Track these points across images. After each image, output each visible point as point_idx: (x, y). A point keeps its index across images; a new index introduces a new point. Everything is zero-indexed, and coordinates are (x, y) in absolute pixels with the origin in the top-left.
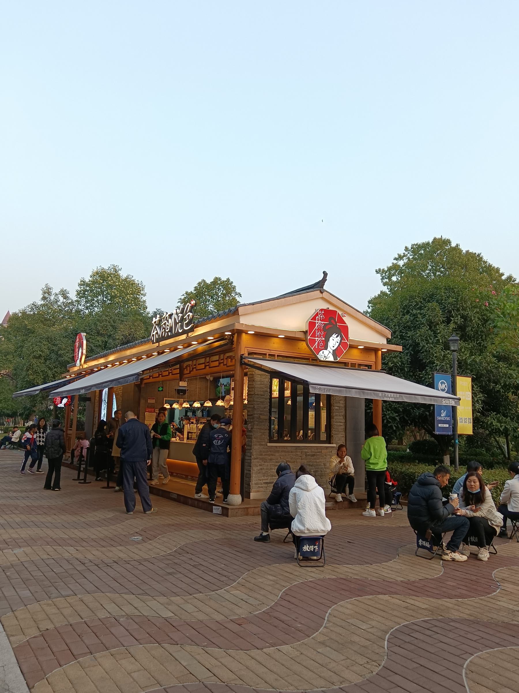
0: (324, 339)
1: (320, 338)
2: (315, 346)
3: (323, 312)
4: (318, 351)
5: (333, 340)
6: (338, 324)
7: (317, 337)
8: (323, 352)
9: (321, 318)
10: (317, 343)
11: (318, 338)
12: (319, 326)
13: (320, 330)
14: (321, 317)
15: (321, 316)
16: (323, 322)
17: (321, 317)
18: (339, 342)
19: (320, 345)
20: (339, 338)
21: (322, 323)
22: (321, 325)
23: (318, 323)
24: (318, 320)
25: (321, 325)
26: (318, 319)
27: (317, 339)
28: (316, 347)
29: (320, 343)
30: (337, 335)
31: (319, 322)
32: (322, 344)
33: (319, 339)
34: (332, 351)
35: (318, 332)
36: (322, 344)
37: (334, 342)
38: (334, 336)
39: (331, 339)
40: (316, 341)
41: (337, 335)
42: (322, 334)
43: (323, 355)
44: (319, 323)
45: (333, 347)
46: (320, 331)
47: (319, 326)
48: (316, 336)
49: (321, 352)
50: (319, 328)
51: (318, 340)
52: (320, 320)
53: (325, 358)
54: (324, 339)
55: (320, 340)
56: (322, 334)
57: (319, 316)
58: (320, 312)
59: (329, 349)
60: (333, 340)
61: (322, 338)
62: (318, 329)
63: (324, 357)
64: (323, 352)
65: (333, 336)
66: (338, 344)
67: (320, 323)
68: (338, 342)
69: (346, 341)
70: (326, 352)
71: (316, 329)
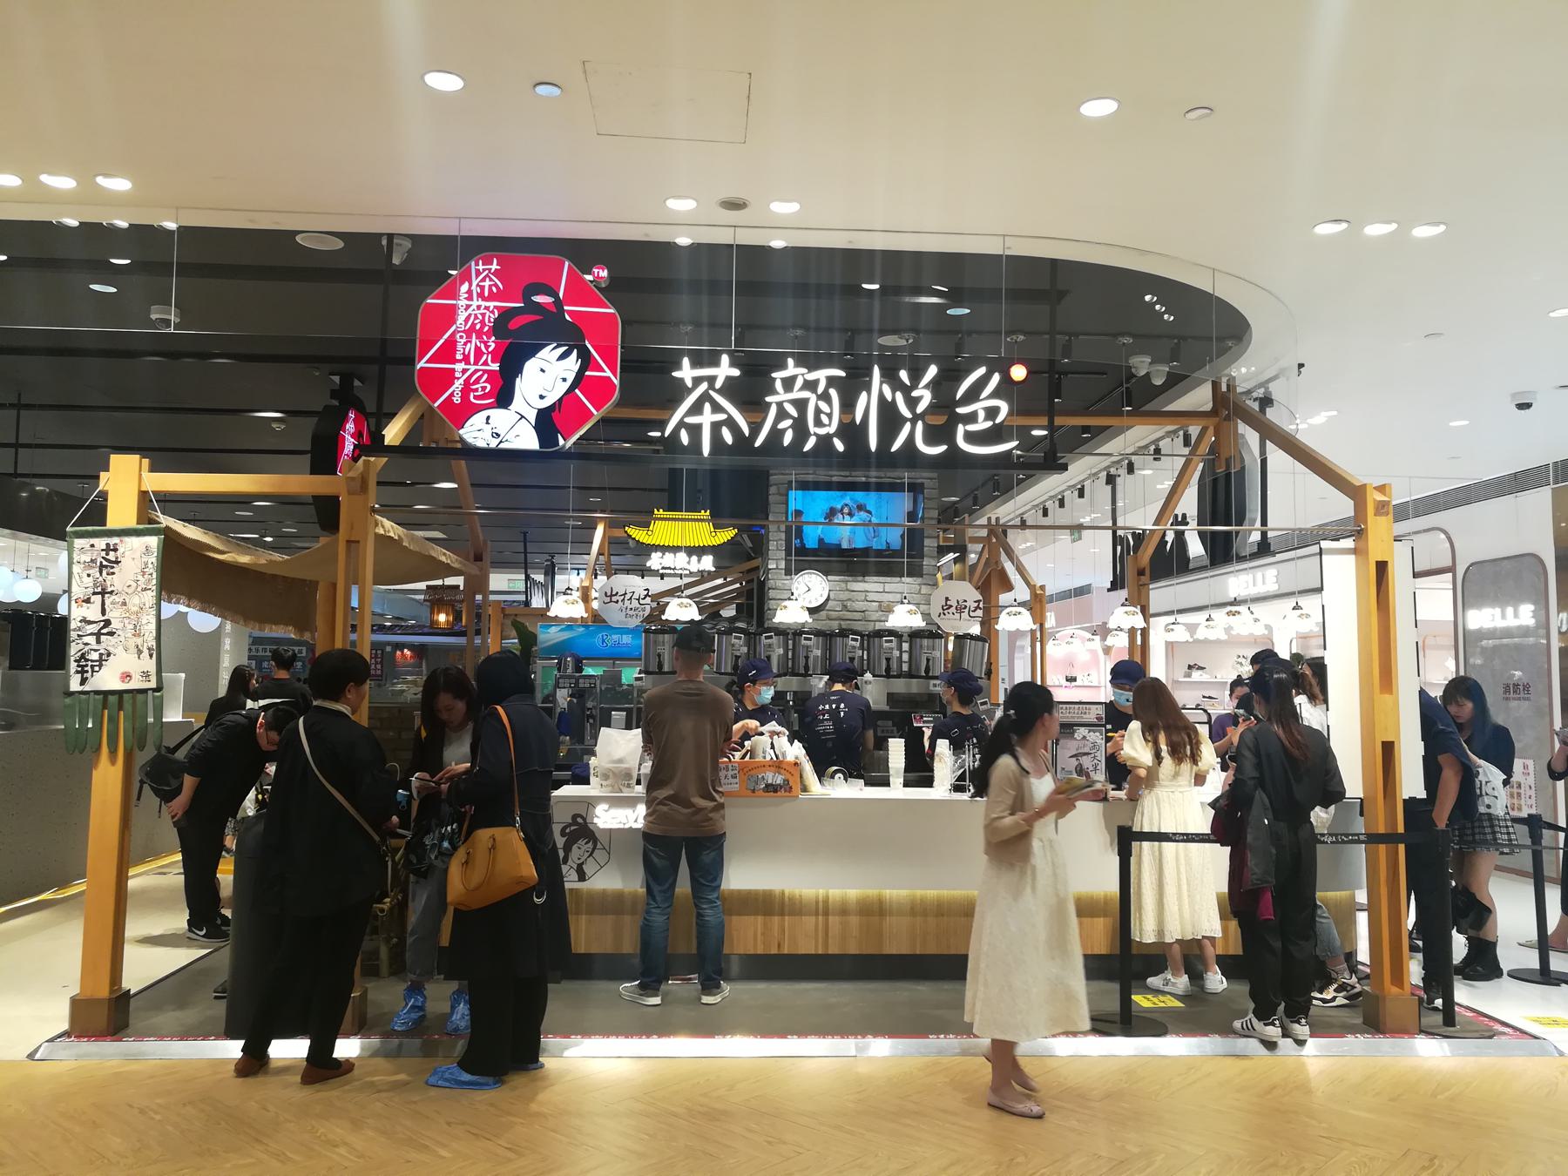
0: (495, 367)
1: (476, 363)
2: (452, 394)
3: (494, 267)
4: (463, 412)
5: (542, 371)
6: (566, 308)
7: (460, 361)
8: (488, 418)
9: (482, 288)
11: (468, 363)
12: (476, 317)
13: (479, 334)
14: (487, 283)
15: (483, 280)
16: (492, 304)
17: (487, 283)
18: (571, 377)
19: (476, 390)
20: (572, 364)
21: (487, 308)
22: (483, 315)
23: (468, 307)
24: (470, 298)
26: (470, 292)
27: (459, 367)
28: (457, 399)
29: (477, 381)
30: (564, 348)
31: (475, 303)
32: (484, 388)
33: (473, 368)
34: (532, 416)
36: (484, 388)
37: (546, 380)
38: (549, 354)
39: (531, 366)
40: (457, 375)
41: (564, 348)
42: (487, 347)
43: (488, 429)
44: (474, 307)
45: (542, 397)
47: (476, 317)
48: (459, 357)
49: (477, 420)
50: (474, 325)
51: (464, 371)
54: (495, 367)
55: (476, 371)
56: (487, 347)
57: (475, 283)
58: (481, 267)
59: (518, 403)
60: (542, 371)
61: (485, 363)
62: (469, 333)
64: (488, 418)
66: (567, 385)
67: (479, 307)
68: (564, 380)
69: (608, 373)
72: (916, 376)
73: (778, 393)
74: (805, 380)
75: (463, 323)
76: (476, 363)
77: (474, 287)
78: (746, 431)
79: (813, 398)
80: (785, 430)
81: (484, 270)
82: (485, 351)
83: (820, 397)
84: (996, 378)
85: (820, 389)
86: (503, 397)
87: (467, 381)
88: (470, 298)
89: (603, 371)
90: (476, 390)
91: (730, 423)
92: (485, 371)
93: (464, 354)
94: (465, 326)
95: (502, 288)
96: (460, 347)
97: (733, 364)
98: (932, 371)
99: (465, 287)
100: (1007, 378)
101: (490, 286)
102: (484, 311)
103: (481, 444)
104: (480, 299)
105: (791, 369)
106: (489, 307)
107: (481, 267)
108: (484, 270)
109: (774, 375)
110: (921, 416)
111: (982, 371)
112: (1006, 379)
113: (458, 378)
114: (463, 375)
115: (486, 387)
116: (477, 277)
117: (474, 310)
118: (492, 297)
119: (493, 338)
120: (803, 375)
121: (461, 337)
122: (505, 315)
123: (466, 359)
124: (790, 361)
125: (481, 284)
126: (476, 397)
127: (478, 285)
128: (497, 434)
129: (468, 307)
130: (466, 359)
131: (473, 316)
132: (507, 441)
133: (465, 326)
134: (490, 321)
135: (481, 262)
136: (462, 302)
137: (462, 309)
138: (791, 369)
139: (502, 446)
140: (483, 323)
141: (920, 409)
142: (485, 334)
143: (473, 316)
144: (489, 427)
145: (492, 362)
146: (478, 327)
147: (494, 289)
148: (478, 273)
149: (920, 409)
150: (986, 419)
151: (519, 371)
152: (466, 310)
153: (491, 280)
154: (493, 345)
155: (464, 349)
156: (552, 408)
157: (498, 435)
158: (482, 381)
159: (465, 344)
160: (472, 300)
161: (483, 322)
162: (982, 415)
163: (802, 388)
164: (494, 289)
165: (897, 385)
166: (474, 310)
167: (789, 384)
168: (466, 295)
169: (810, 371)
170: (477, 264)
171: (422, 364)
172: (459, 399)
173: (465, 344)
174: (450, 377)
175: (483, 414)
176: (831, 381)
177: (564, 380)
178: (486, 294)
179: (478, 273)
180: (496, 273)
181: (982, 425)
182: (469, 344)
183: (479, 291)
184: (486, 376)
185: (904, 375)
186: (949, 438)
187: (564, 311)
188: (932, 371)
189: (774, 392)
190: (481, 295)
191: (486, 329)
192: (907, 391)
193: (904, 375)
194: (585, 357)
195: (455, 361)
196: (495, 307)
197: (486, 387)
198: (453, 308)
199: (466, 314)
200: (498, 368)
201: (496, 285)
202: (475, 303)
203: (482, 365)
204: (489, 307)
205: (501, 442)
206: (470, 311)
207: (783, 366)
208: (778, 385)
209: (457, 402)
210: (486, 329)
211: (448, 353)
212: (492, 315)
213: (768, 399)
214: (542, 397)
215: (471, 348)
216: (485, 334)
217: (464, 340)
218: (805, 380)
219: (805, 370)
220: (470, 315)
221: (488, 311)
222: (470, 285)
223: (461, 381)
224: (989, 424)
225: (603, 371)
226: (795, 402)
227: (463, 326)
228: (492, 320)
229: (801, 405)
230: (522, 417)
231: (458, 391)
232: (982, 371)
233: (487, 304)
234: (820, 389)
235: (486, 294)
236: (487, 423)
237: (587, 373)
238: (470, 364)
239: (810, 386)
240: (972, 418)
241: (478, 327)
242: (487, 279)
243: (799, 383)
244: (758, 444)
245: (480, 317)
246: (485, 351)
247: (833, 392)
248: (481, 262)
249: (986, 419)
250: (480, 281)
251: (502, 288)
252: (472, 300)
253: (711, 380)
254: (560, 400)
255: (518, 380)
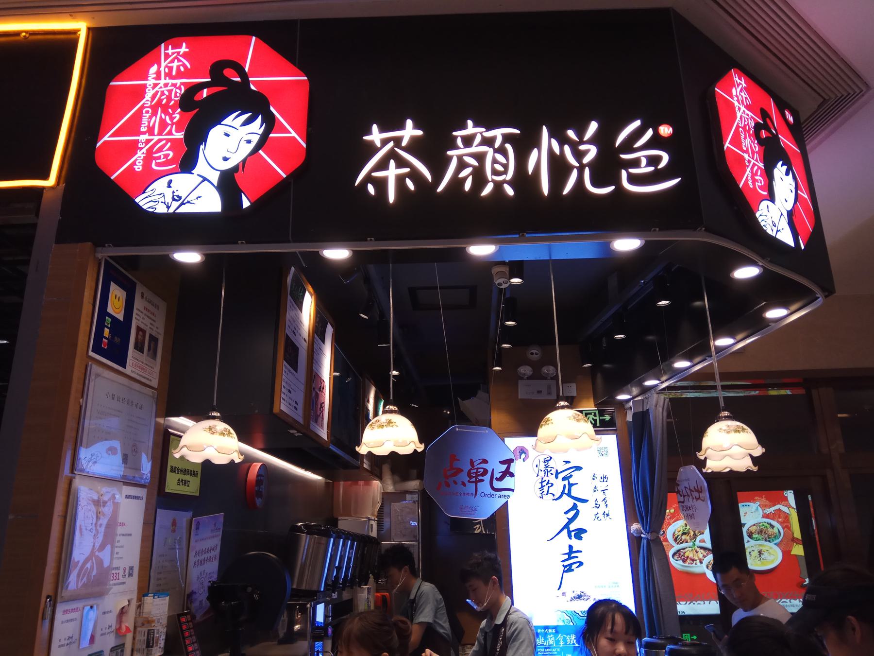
1: (160, 134)
2: (134, 163)
5: (227, 135)
7: (144, 133)
8: (170, 182)
9: (171, 69)
10: (140, 154)
12: (163, 93)
14: (176, 64)
15: (172, 61)
16: (178, 82)
17: (176, 64)
19: (159, 158)
20: (257, 127)
21: (174, 85)
23: (155, 85)
25: (170, 91)
27: (143, 138)
28: (139, 167)
29: (160, 150)
33: (156, 138)
34: (215, 177)
35: (154, 114)
36: (166, 156)
38: (234, 120)
39: (216, 134)
40: (140, 145)
44: (162, 85)
45: (226, 159)
46: (166, 112)
47: (163, 93)
48: (143, 129)
49: (160, 185)
50: (160, 100)
51: (148, 141)
52: (166, 75)
53: (175, 204)
55: (160, 141)
56: (172, 119)
57: (163, 64)
59: (201, 167)
60: (227, 135)
61: (170, 133)
63: (169, 199)
65: (228, 120)
66: (251, 146)
67: (166, 85)
69: (293, 134)
70: (183, 183)
71: (143, 107)
72: (580, 133)
73: (458, 148)
74: (483, 137)
75: (150, 99)
76: (160, 134)
77: (162, 69)
78: (428, 176)
79: (490, 151)
80: (465, 178)
81: (173, 53)
82: (170, 122)
83: (496, 151)
84: (650, 133)
85: (497, 144)
86: (187, 163)
87: (150, 152)
88: (158, 76)
89: (290, 133)
90: (159, 158)
91: (415, 175)
92: (168, 141)
93: (148, 126)
94: (152, 102)
95: (189, 66)
96: (145, 121)
97: (416, 126)
98: (593, 126)
99: (154, 69)
100: (656, 133)
101: (178, 67)
102: (172, 88)
103: (161, 209)
104: (167, 78)
105: (471, 128)
106: (176, 84)
107: (170, 51)
108: (173, 53)
109: (455, 133)
110: (588, 165)
111: (637, 123)
112: (656, 133)
113: (141, 149)
114: (146, 145)
115: (169, 155)
116: (165, 60)
117: (161, 88)
118: (179, 75)
119: (179, 110)
120: (481, 133)
121: (147, 112)
122: (193, 90)
123: (150, 131)
124: (470, 123)
125: (169, 65)
126: (158, 165)
127: (167, 66)
128: (178, 196)
129: (155, 85)
130: (150, 131)
131: (159, 94)
132: (188, 202)
133: (152, 102)
134: (176, 96)
135: (170, 47)
136: (151, 82)
137: (150, 88)
138: (471, 128)
139: (183, 210)
140: (169, 98)
141: (587, 160)
142: (170, 107)
143: (159, 94)
144: (171, 190)
145: (177, 131)
146: (164, 102)
147: (182, 69)
148: (167, 56)
149: (587, 160)
150: (648, 165)
151: (204, 139)
152: (153, 88)
153: (179, 61)
154: (178, 117)
155: (149, 122)
156: (235, 169)
157: (180, 198)
158: (164, 150)
159: (150, 118)
160: (160, 79)
161: (169, 98)
162: (644, 162)
163: (479, 145)
164: (182, 69)
165: (563, 140)
166: (161, 88)
167: (468, 141)
168: (155, 76)
169: (488, 130)
170: (166, 48)
171: (106, 138)
172: (141, 167)
173: (150, 118)
174: (134, 147)
175: (166, 179)
176: (507, 138)
177: (249, 142)
178: (174, 73)
179: (167, 56)
180: (185, 55)
181: (644, 169)
182: (154, 118)
183: (167, 70)
184: (169, 144)
185: (571, 133)
186: (617, 181)
187: (249, 81)
188: (593, 126)
189: (457, 148)
190: (169, 75)
191: (173, 102)
192: (574, 146)
193: (571, 133)
194: (270, 123)
195: (140, 133)
196: (182, 84)
197: (169, 155)
198: (145, 86)
199: (153, 92)
200: (182, 137)
201: (184, 65)
202: (162, 82)
203: (166, 135)
204: (176, 84)
205: (183, 204)
206: (156, 89)
207: (464, 127)
208: (459, 142)
209: (137, 170)
210: (173, 102)
211: (133, 127)
212: (178, 91)
213: (449, 153)
214: (226, 159)
215: (156, 121)
216: (170, 107)
217: (148, 115)
218: (483, 137)
219: (484, 130)
220: (157, 92)
221: (176, 87)
222: (159, 66)
223: (144, 150)
224: (651, 169)
225: (290, 133)
226: (474, 156)
227: (149, 103)
228: (178, 95)
229: (480, 157)
230: (205, 179)
231: (140, 160)
232: (637, 123)
233: (174, 81)
234: (497, 144)
235: (174, 73)
236: (169, 186)
237: (271, 135)
238: (154, 135)
239: (488, 142)
240: (636, 163)
241: (164, 102)
242: (176, 61)
243: (478, 139)
244: (440, 189)
245: (167, 93)
246: (170, 122)
247: (508, 146)
248: (170, 47)
249: (648, 165)
250: (169, 63)
251: (189, 66)
252: (160, 79)
253: (398, 141)
254: (244, 162)
255: (202, 147)
